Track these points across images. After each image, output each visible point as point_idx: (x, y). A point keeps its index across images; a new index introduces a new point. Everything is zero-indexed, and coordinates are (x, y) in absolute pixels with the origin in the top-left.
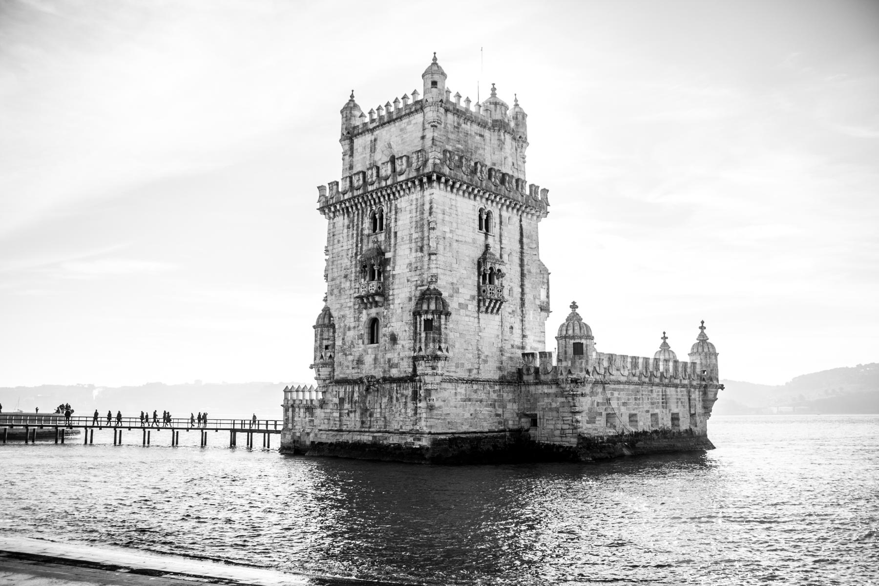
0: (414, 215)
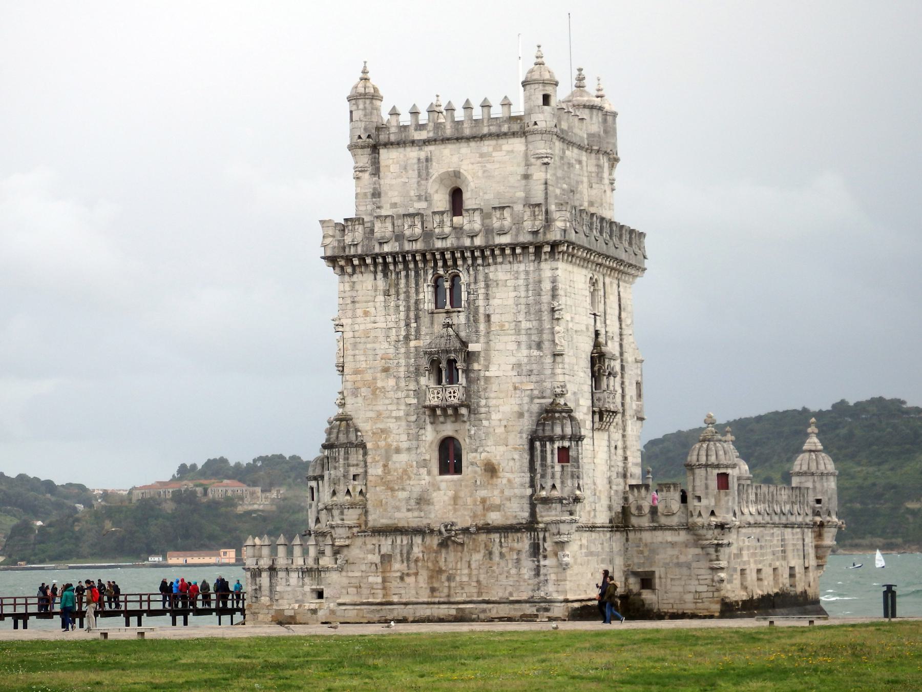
0: (523, 294)
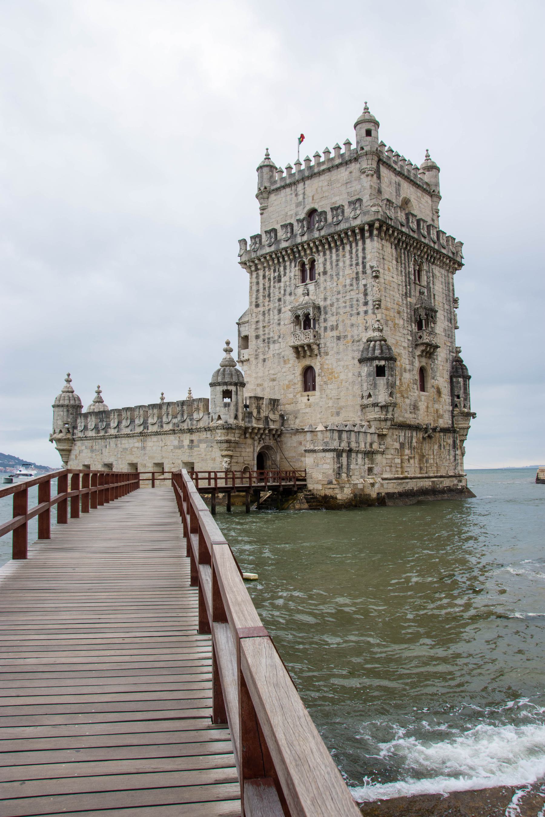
0: (444, 288)
